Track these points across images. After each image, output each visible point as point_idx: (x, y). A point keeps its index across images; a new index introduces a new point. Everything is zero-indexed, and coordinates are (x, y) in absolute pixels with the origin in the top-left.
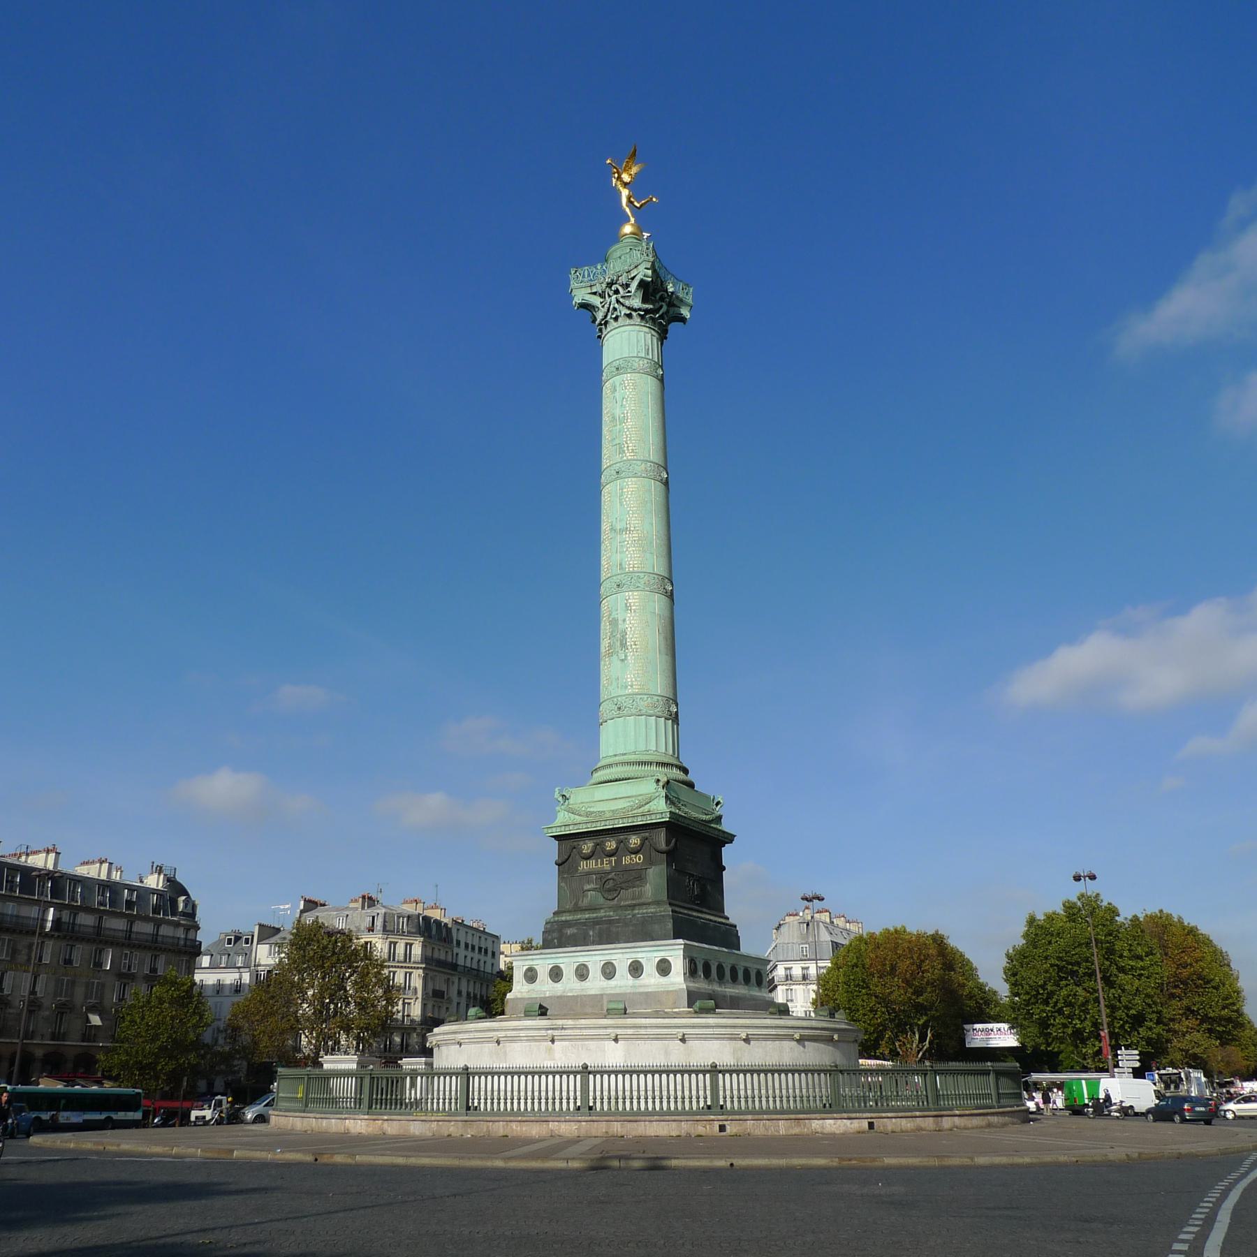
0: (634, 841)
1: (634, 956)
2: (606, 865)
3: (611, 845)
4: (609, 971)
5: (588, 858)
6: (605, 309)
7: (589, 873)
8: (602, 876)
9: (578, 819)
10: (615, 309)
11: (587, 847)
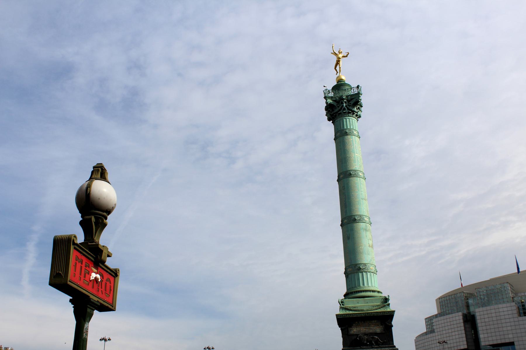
6: (339, 108)
9: (351, 312)
10: (344, 109)
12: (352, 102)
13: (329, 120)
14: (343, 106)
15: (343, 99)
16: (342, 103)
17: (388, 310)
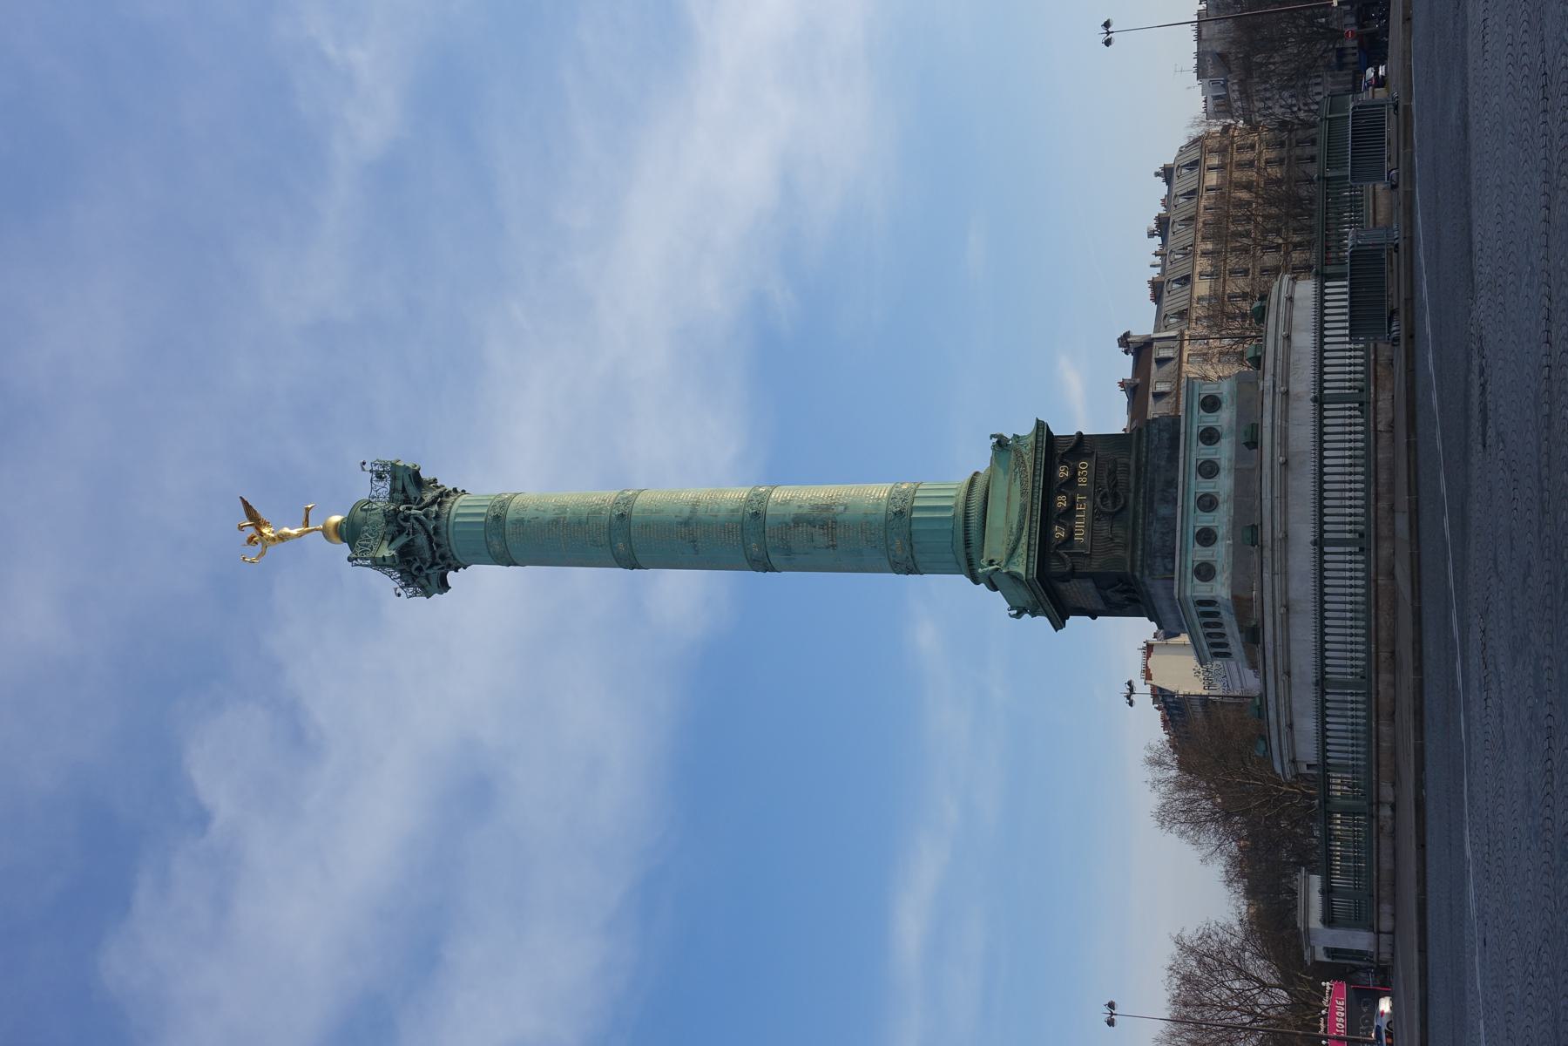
0: (1063, 473)
1: (1195, 437)
2: (1083, 508)
3: (1062, 502)
4: (1209, 470)
5: (1071, 534)
7: (1091, 530)
8: (1097, 515)
9: (1024, 540)
11: (1059, 533)
12: (412, 491)
13: (444, 586)
14: (417, 519)
15: (396, 512)
16: (406, 519)
17: (1032, 439)
